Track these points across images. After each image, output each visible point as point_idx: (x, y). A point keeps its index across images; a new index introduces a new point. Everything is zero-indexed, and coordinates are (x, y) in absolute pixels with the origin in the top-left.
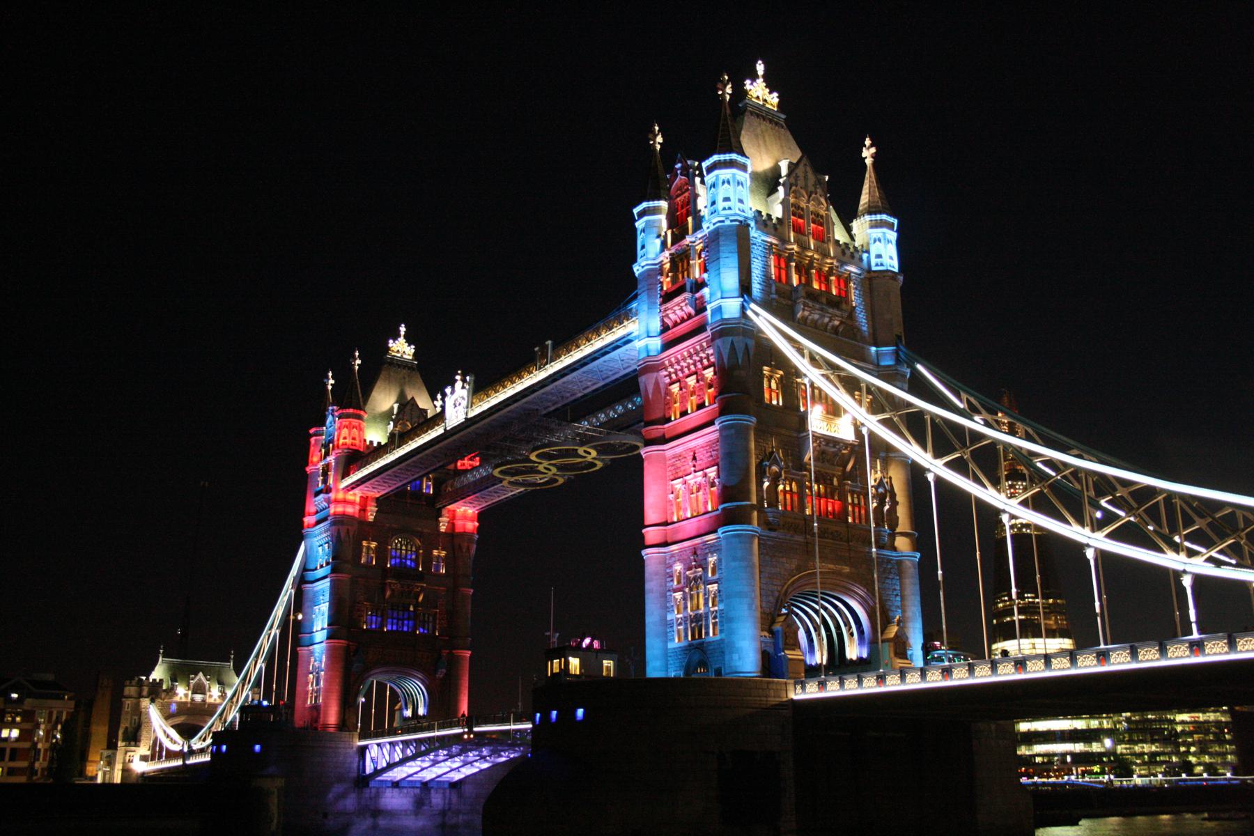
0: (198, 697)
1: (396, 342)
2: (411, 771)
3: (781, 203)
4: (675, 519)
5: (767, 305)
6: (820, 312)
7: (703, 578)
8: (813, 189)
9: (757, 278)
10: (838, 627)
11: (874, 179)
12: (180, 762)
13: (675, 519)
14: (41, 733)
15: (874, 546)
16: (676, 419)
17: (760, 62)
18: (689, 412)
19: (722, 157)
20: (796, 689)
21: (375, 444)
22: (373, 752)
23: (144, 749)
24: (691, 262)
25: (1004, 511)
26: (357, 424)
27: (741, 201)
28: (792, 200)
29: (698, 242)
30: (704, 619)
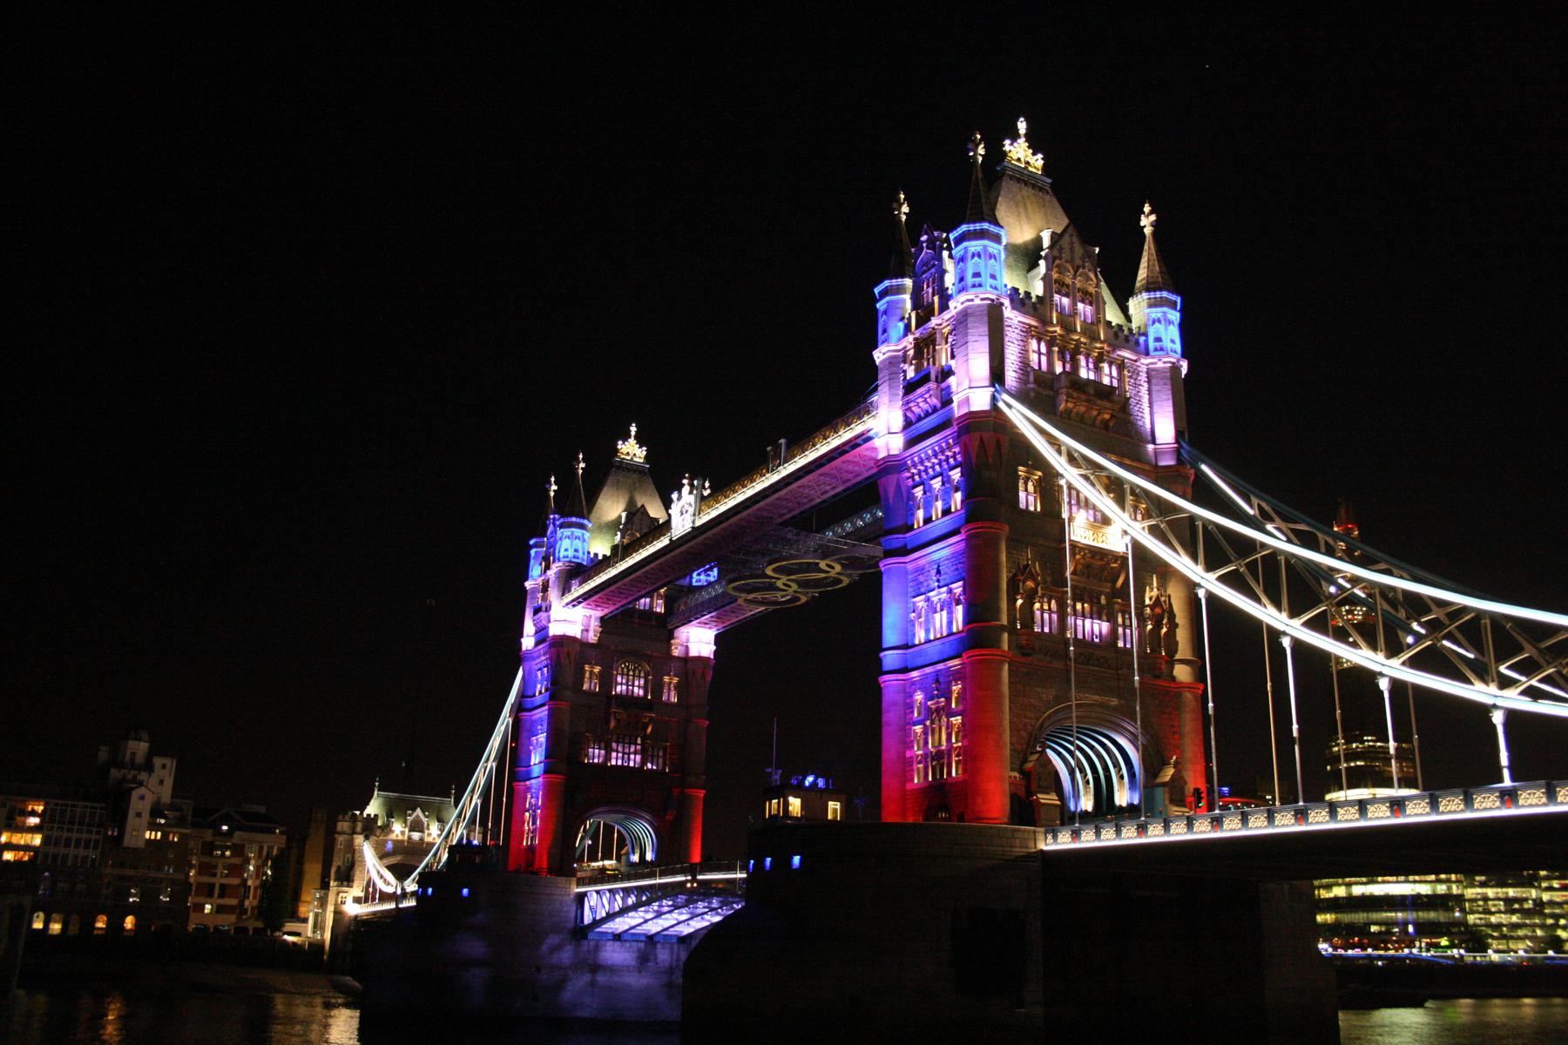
0: (416, 836)
1: (626, 443)
2: (634, 922)
3: (1042, 279)
5: (1023, 396)
6: (1087, 404)
8: (1080, 263)
10: (1106, 769)
11: (1153, 251)
12: (392, 906)
13: (917, 642)
14: (251, 868)
15: (1136, 673)
17: (1022, 119)
18: (934, 519)
19: (972, 227)
20: (1046, 838)
21: (600, 557)
22: (592, 900)
23: (357, 890)
24: (937, 347)
25: (1285, 633)
26: (580, 535)
27: (993, 277)
28: (1055, 276)
30: (946, 756)
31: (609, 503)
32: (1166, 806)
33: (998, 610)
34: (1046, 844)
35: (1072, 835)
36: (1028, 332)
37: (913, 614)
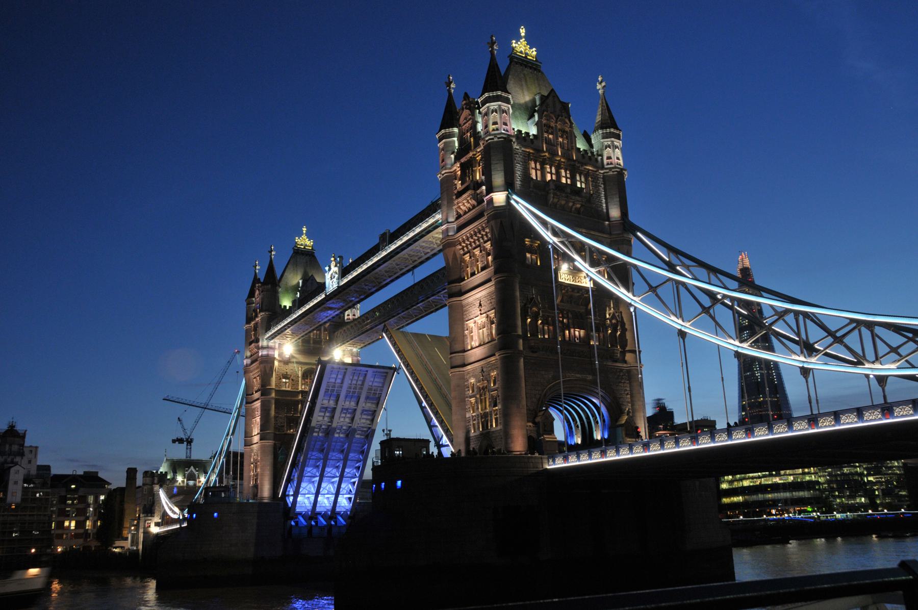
0: (191, 483)
3: (536, 124)
4: (469, 348)
6: (566, 199)
9: (519, 178)
10: (588, 418)
14: (91, 509)
15: (597, 359)
16: (468, 278)
18: (476, 273)
20: (549, 461)
21: (288, 308)
23: (157, 519)
27: (505, 124)
28: (544, 122)
30: (489, 416)
31: (292, 275)
32: (623, 438)
33: (515, 327)
34: (549, 465)
35: (563, 459)
36: (527, 158)
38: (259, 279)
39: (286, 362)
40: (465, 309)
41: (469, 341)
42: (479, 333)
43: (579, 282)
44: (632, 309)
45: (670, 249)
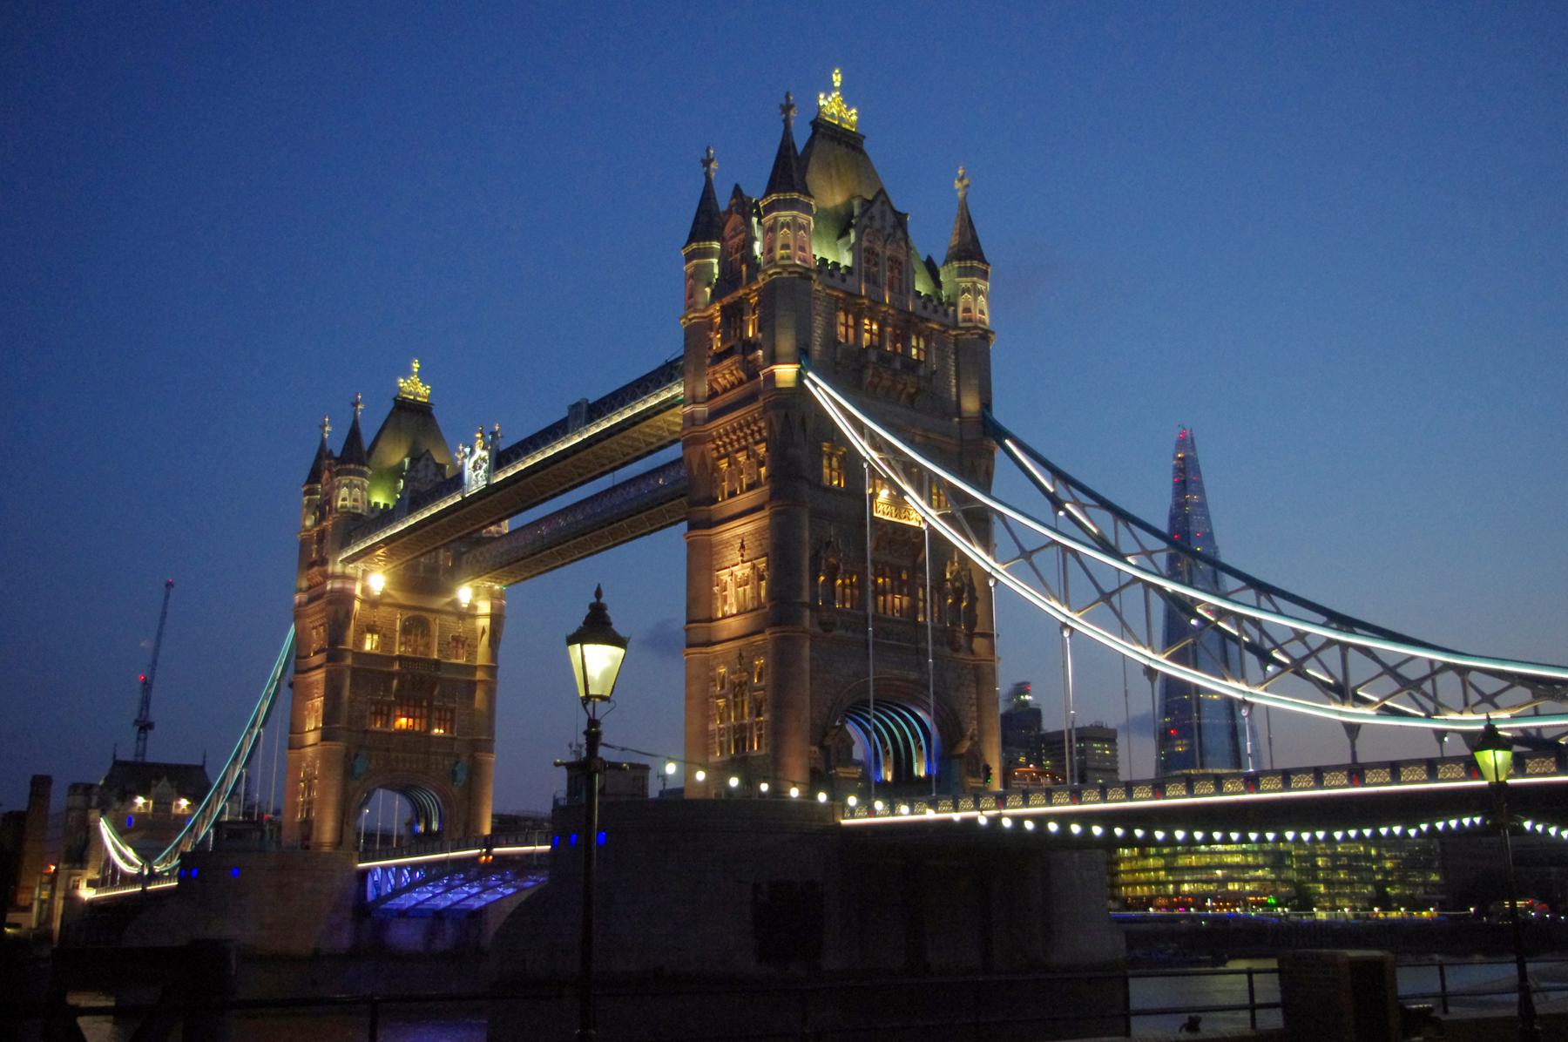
4: (720, 616)
7: (748, 683)
8: (892, 231)
9: (819, 339)
15: (930, 655)
16: (723, 500)
17: (837, 71)
18: (738, 492)
21: (382, 507)
24: (745, 318)
26: (359, 483)
27: (802, 249)
28: (865, 244)
29: (753, 295)
34: (844, 818)
37: (717, 588)
38: (331, 451)
39: (372, 603)
40: (715, 549)
41: (719, 604)
42: (737, 592)
43: (905, 517)
44: (991, 583)
45: (1057, 474)
